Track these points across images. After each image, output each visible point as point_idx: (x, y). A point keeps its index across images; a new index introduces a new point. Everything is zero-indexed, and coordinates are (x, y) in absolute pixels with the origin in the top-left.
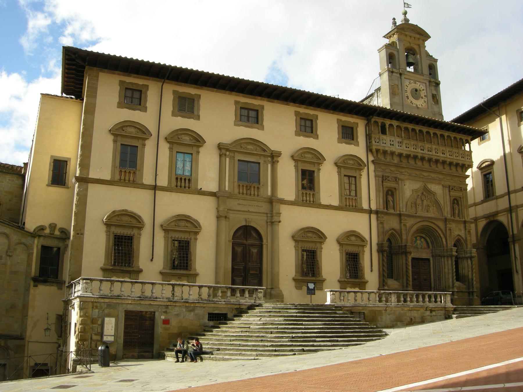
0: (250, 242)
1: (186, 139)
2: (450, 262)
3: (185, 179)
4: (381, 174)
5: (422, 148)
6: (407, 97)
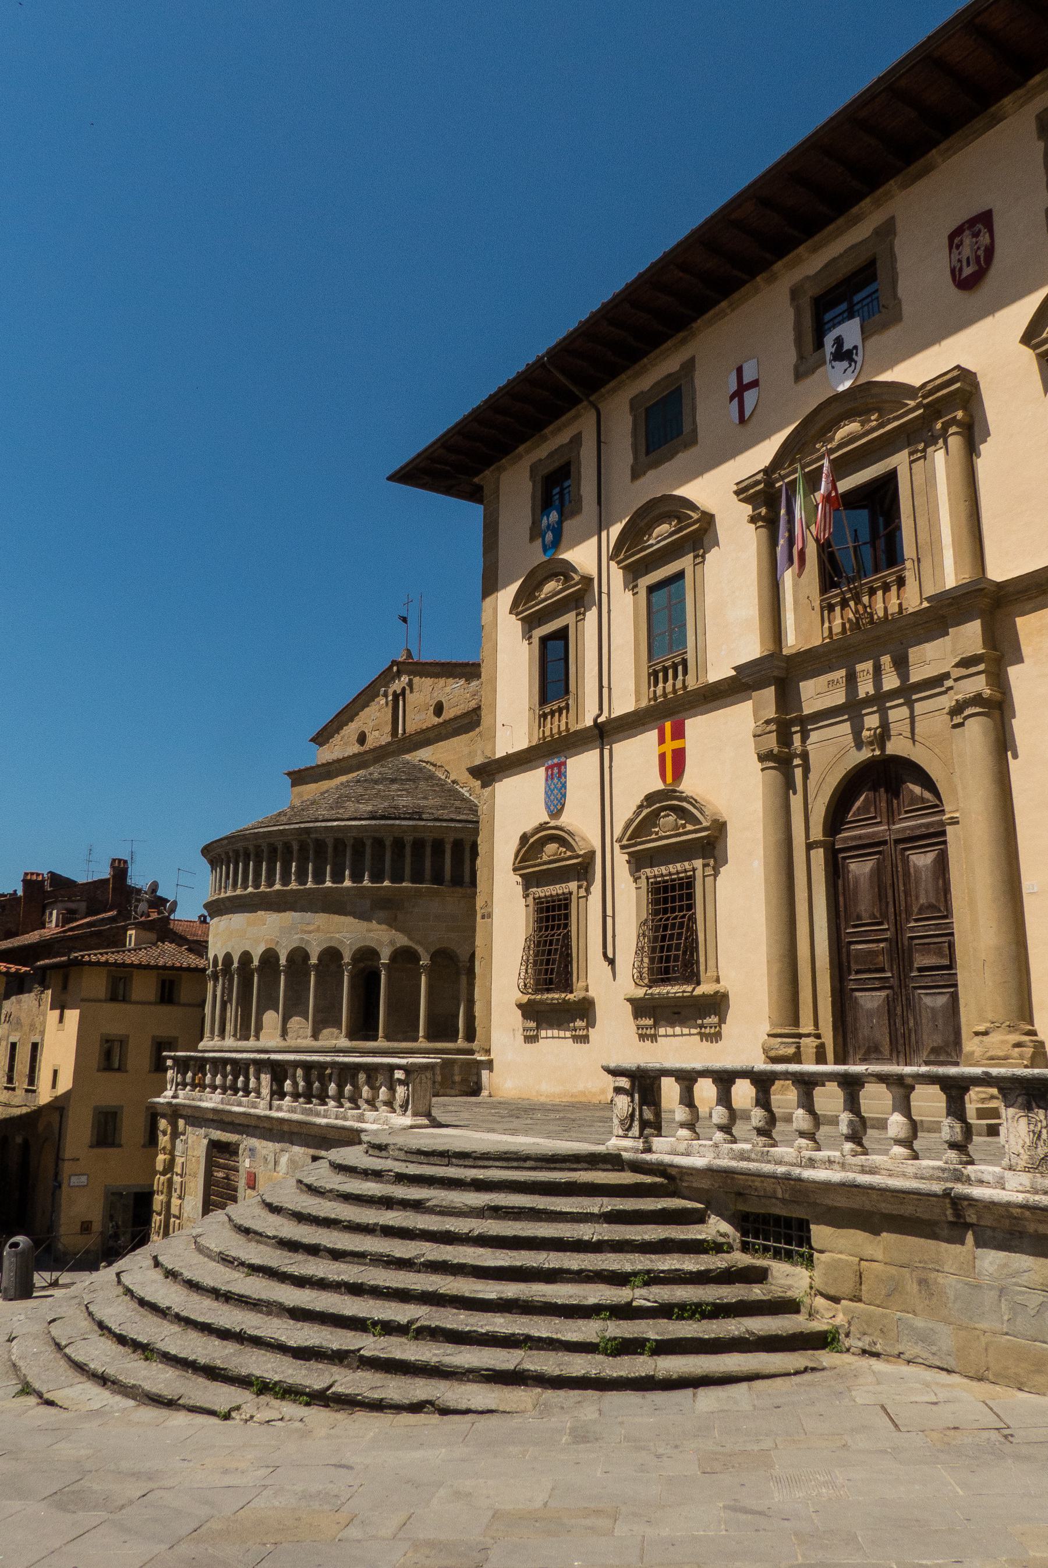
0: (905, 825)
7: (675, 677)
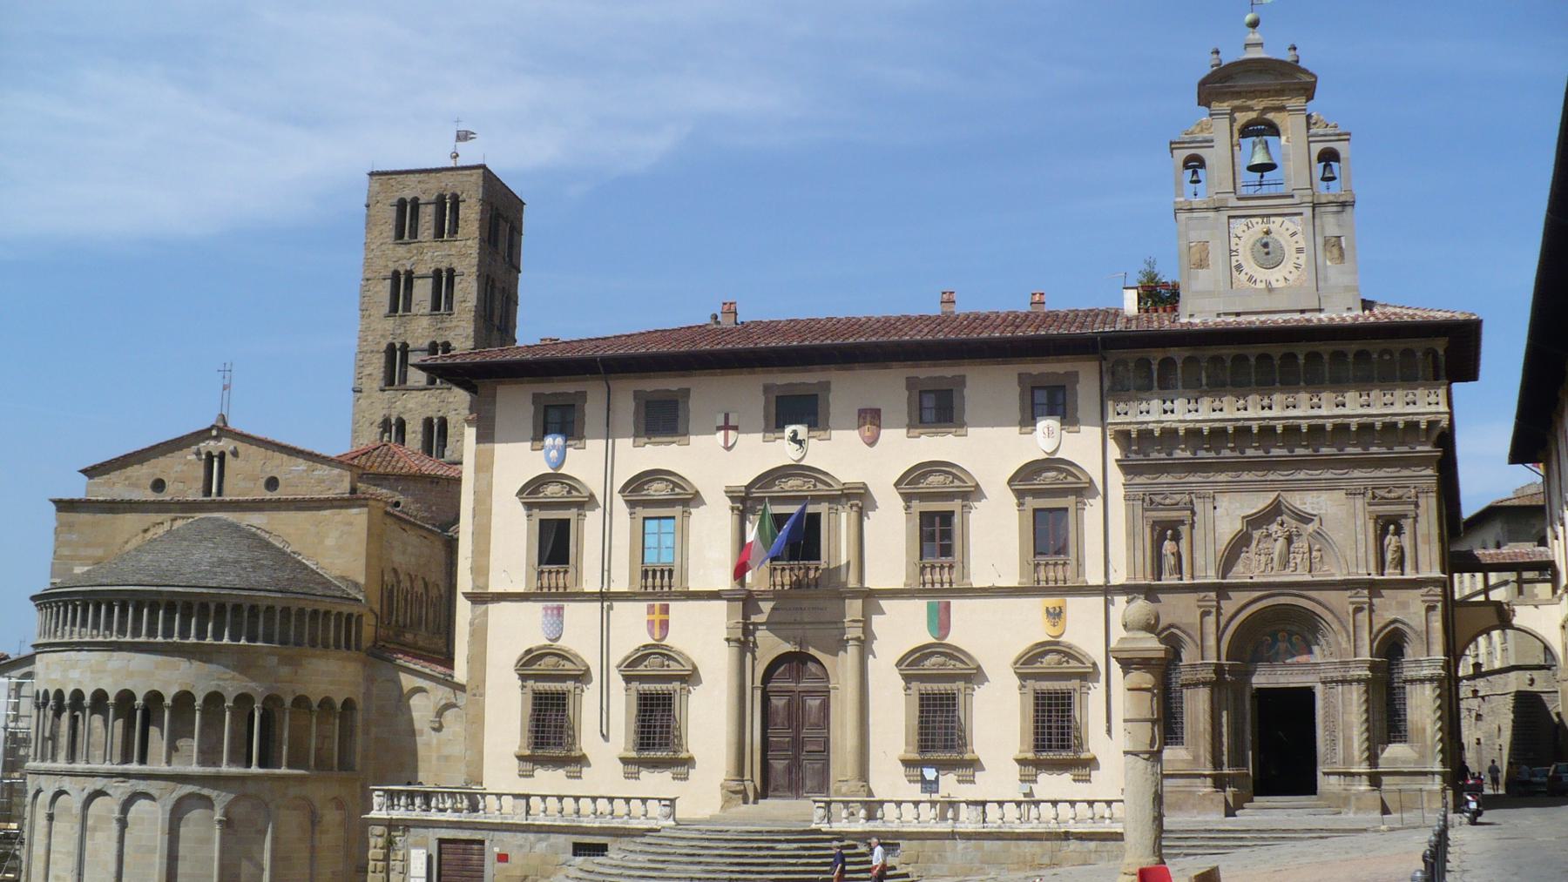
0: (805, 685)
1: (657, 490)
2: (1355, 696)
3: (662, 572)
4: (1140, 491)
6: (1239, 268)
7: (662, 578)
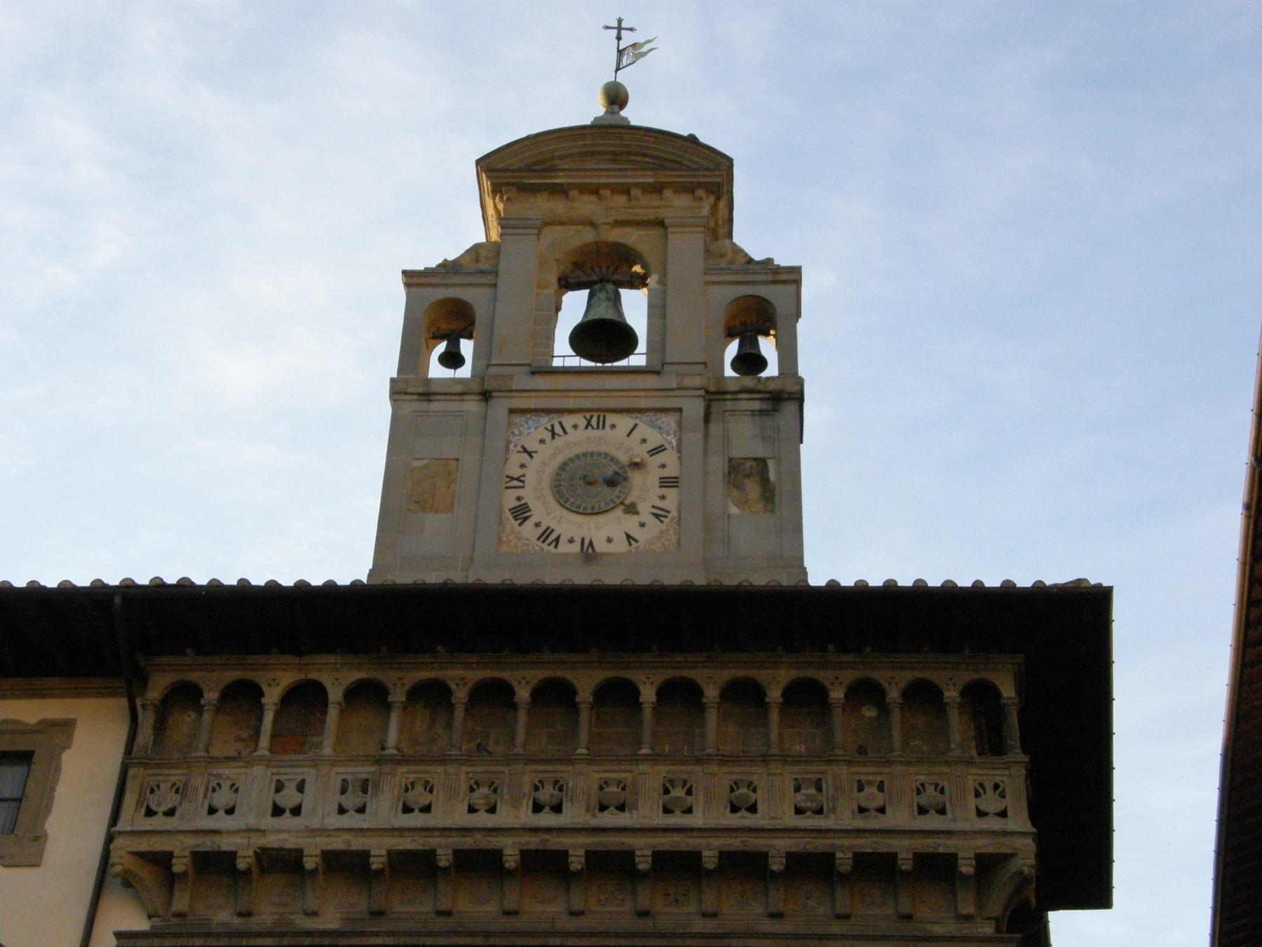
5: (547, 794)
6: (521, 513)
